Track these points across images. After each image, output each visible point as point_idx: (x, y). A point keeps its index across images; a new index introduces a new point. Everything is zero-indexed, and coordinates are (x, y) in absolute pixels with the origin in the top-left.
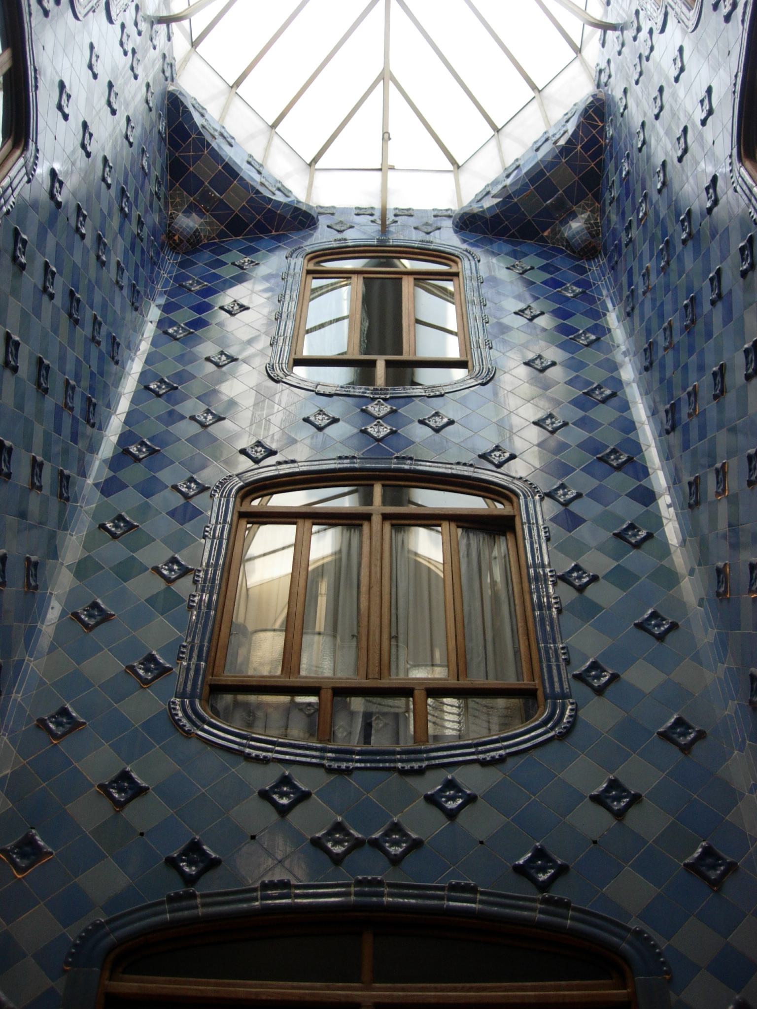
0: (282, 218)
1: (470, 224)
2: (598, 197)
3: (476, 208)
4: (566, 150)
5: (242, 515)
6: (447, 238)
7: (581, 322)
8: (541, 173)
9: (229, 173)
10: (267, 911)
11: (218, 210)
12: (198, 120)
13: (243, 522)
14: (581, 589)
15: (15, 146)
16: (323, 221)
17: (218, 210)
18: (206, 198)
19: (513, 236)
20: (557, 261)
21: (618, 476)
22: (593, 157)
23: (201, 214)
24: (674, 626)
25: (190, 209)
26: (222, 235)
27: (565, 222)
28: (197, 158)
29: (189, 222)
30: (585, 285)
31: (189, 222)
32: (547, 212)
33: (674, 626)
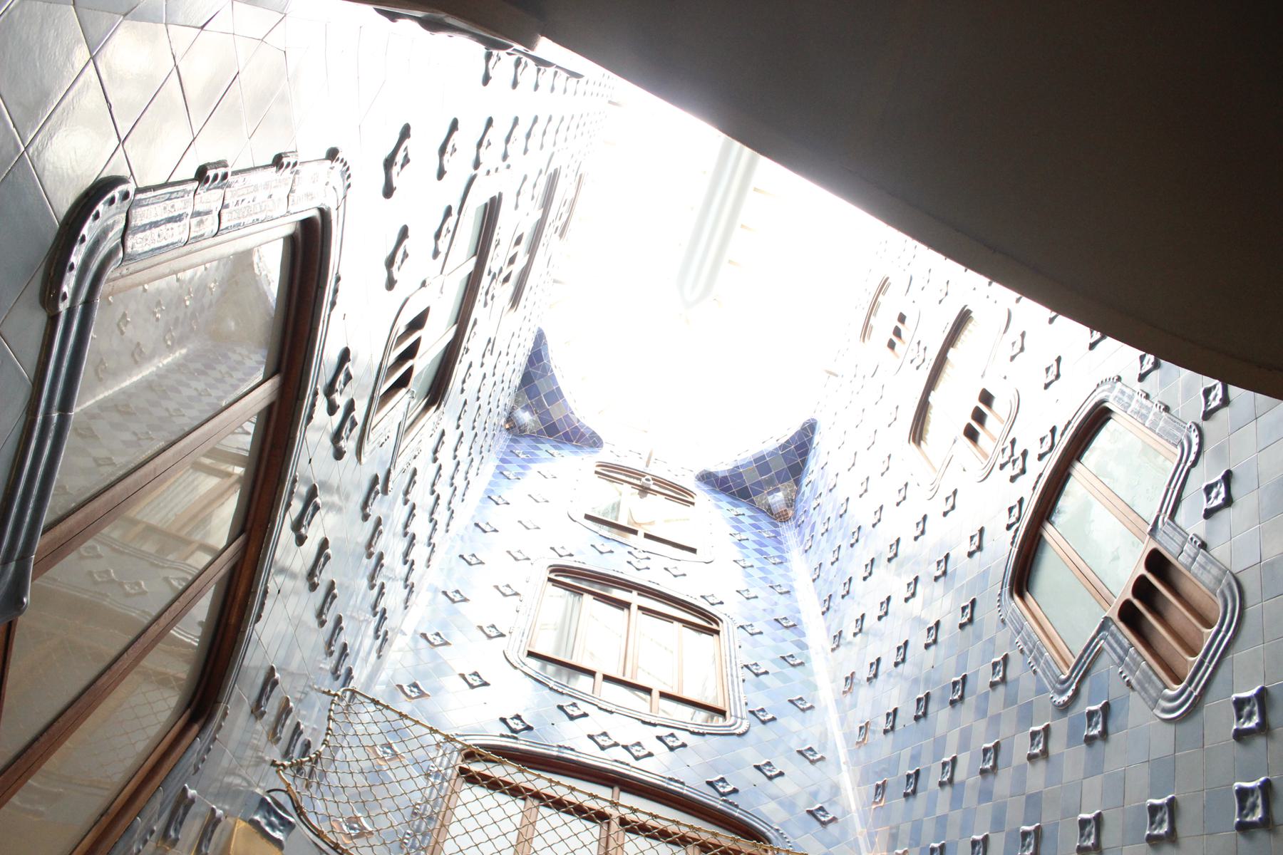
0: (583, 435)
1: (708, 479)
2: (798, 482)
3: (712, 470)
4: (783, 447)
5: (550, 580)
6: (690, 483)
7: (770, 550)
8: (763, 457)
9: (556, 395)
10: (558, 758)
11: (543, 416)
12: (551, 355)
13: (550, 584)
14: (757, 675)
15: (512, 306)
16: (606, 448)
17: (543, 416)
18: (540, 404)
19: (733, 494)
20: (761, 516)
21: (788, 632)
22: (800, 455)
23: (532, 413)
24: (811, 707)
25: (527, 408)
26: (540, 432)
27: (769, 493)
28: (542, 376)
29: (525, 417)
30: (778, 534)
31: (525, 417)
32: (759, 484)
33: (811, 707)
